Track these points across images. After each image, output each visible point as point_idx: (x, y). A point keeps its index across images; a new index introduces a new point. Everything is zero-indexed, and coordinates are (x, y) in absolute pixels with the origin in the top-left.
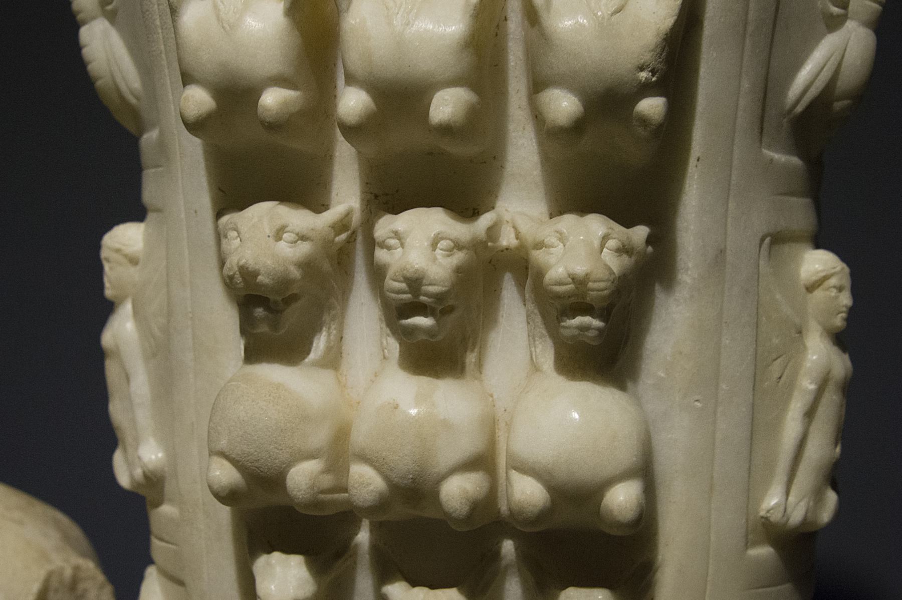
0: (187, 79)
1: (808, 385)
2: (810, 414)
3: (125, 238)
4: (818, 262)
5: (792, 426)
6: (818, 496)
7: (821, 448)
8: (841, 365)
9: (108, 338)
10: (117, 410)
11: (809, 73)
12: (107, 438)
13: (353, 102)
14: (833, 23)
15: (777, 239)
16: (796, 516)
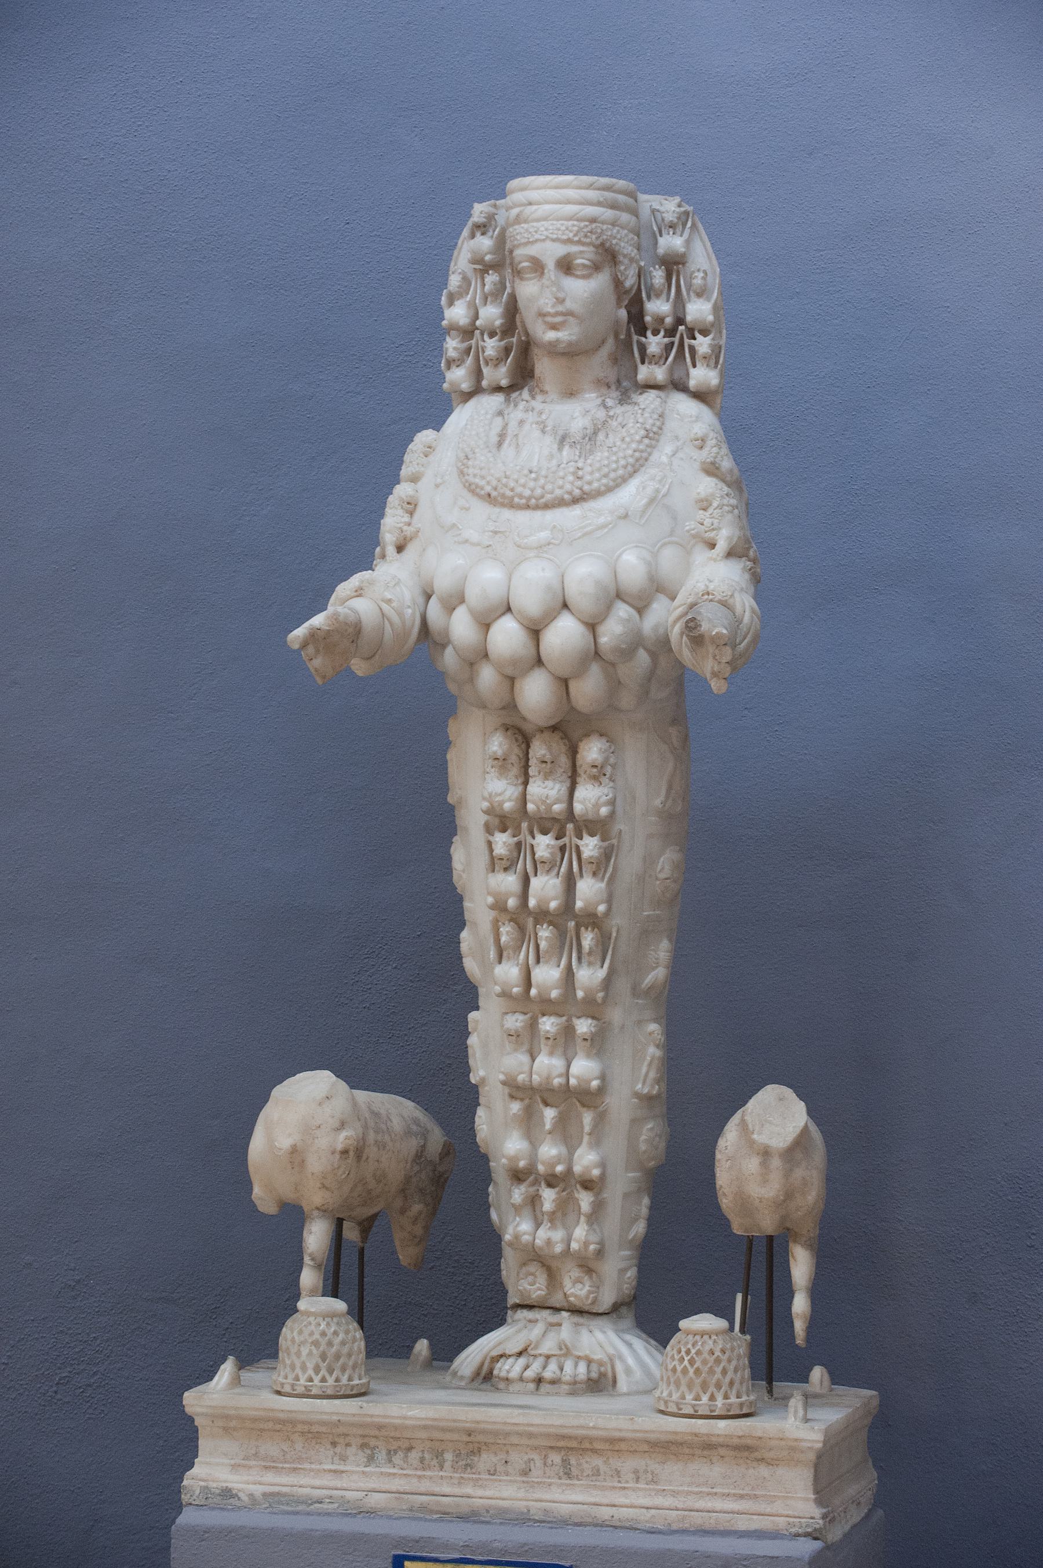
0: (496, 984)
1: (649, 1058)
2: (650, 1065)
3: (473, 1016)
4: (653, 1027)
5: (644, 1069)
6: (653, 1087)
7: (652, 1075)
8: (658, 1053)
9: (469, 1042)
10: (471, 1062)
11: (649, 979)
12: (467, 1070)
13: (533, 992)
14: (654, 969)
15: (639, 1023)
16: (646, 1091)
